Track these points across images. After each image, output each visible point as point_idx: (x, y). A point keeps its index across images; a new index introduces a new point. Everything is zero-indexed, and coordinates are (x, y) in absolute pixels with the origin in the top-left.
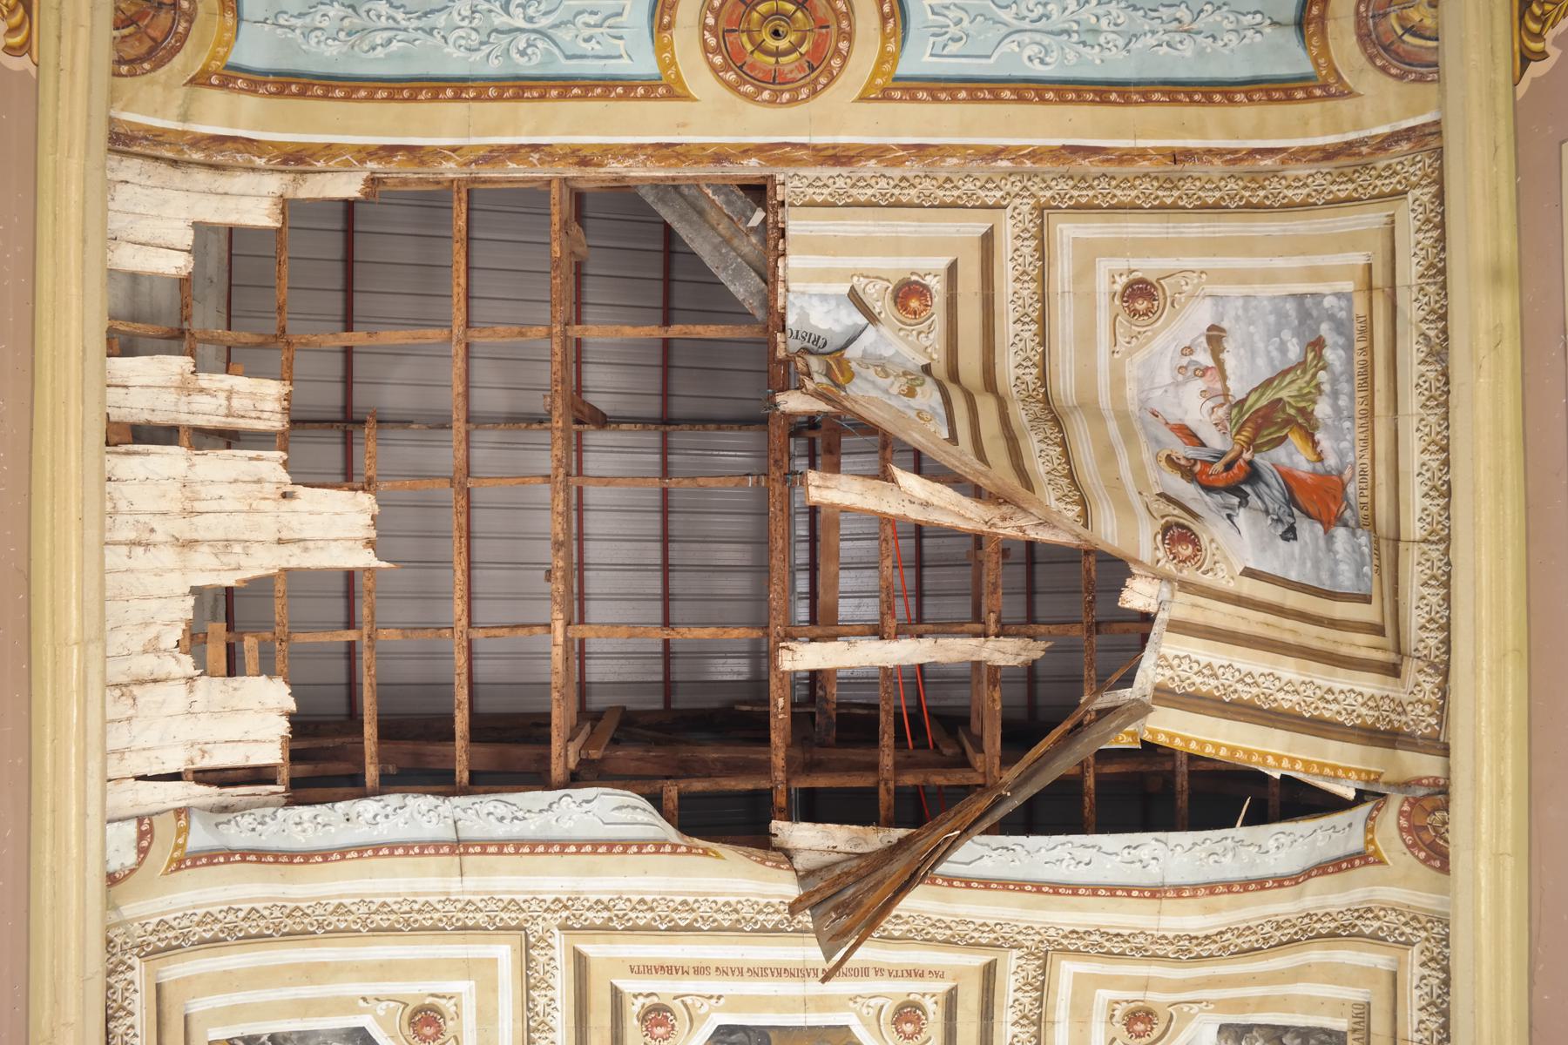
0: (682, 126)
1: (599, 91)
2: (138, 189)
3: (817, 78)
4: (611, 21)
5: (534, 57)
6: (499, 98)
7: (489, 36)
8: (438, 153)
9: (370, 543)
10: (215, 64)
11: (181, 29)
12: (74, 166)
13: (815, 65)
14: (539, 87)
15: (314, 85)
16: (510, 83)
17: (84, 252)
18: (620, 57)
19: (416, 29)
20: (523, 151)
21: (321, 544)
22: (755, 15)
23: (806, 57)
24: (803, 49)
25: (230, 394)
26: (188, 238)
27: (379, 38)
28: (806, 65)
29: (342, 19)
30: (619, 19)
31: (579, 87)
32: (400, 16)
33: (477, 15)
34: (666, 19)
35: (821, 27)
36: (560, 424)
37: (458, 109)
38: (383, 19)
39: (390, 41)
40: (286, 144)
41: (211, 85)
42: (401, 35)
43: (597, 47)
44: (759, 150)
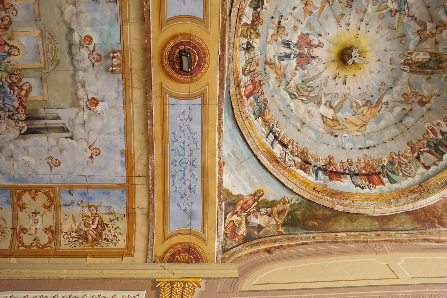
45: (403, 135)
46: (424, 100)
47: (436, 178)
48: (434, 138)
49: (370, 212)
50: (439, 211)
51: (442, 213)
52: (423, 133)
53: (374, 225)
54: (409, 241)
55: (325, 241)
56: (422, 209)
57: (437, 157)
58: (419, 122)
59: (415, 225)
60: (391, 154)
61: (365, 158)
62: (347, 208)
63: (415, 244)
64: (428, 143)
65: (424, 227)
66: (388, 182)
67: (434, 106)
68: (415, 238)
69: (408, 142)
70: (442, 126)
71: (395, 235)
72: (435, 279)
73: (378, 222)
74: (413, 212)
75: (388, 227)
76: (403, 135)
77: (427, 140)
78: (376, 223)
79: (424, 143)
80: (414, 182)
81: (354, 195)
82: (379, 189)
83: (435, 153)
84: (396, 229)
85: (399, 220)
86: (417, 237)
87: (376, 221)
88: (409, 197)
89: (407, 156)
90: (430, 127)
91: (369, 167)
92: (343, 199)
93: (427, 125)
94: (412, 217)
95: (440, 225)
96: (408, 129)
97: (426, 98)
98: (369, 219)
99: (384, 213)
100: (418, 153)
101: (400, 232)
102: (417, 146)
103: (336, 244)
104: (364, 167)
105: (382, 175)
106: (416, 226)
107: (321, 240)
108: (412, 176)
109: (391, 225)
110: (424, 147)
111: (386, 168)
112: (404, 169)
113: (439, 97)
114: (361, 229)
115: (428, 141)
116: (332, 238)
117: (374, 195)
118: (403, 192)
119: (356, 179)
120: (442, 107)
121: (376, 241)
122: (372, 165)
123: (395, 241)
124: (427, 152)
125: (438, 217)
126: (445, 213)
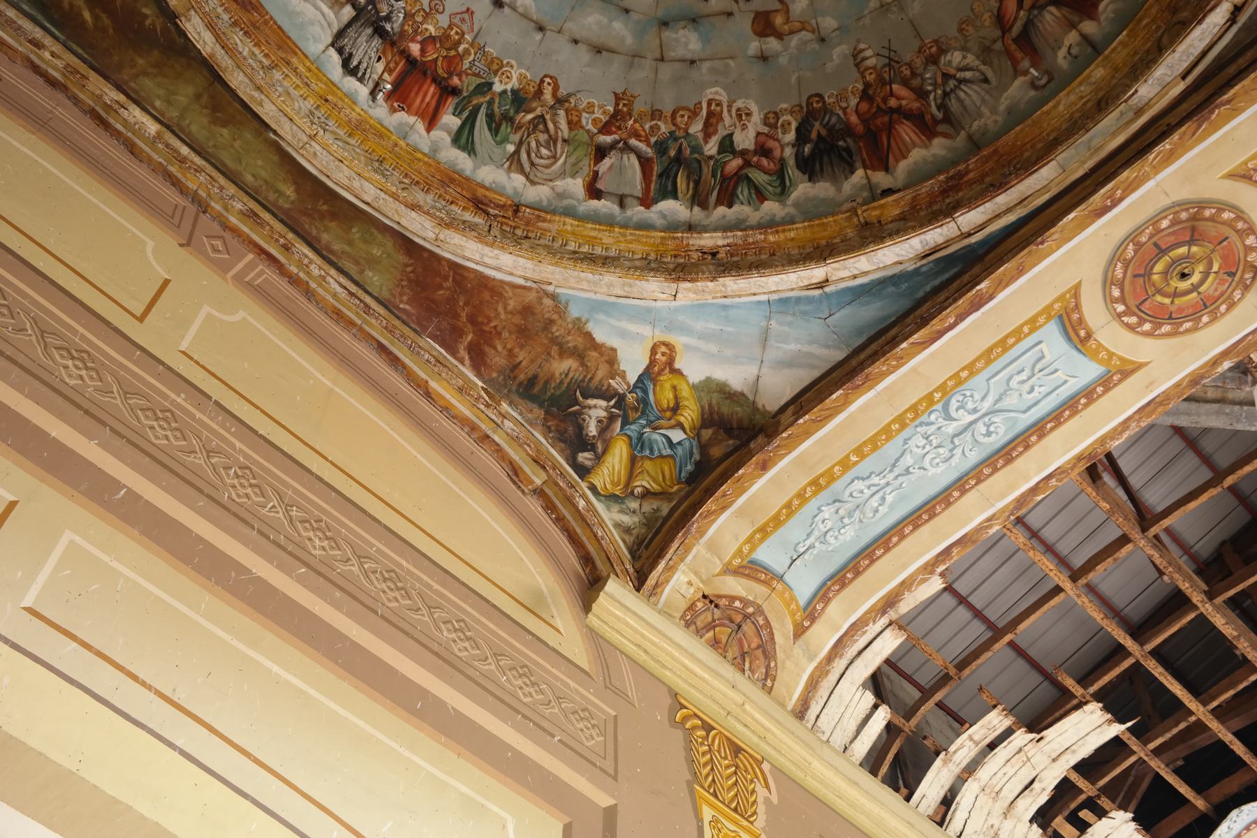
0: (1150, 385)
1: (1067, 413)
2: (825, 711)
3: (1242, 277)
4: (1039, 366)
5: (999, 430)
6: (995, 470)
7: (952, 442)
8: (980, 529)
9: (1110, 722)
10: (798, 617)
11: (761, 622)
12: (816, 765)
13: (1234, 271)
14: (1020, 443)
15: (859, 562)
16: (996, 457)
17: (861, 788)
18: (1066, 382)
19: (896, 478)
20: (1041, 485)
21: (1080, 743)
22: (1155, 277)
23: (1222, 271)
24: (1215, 268)
25: (971, 738)
26: (870, 698)
27: (874, 502)
28: (1225, 276)
29: (837, 512)
30: (1044, 361)
31: (1050, 422)
32: (875, 480)
33: (932, 438)
34: (1082, 333)
35: (1220, 243)
36: (1187, 585)
37: (971, 497)
38: (866, 491)
39: (883, 499)
40: (875, 604)
41: (808, 628)
42: (888, 489)
43: (1042, 389)
44: (1225, 354)
45: (631, 66)
46: (779, 20)
47: (578, 226)
48: (696, 138)
49: (294, 136)
50: (498, 314)
51: (504, 328)
52: (684, 104)
53: (277, 191)
54: (335, 316)
55: (66, 88)
56: (454, 266)
57: (647, 190)
58: (706, 65)
59: (401, 295)
60: (548, 80)
61: (463, 20)
62: (226, 58)
63: (346, 337)
64: (668, 138)
65: (419, 323)
66: (449, 134)
67: (783, 60)
68: (359, 322)
69: (624, 93)
70: (744, 127)
71: (306, 261)
72: (247, 406)
73: (297, 191)
74: (425, 255)
75: (314, 232)
76: (631, 66)
77: (674, 128)
78: (289, 191)
79: (659, 128)
80: (516, 192)
81: (296, 54)
82: (400, 124)
83: (654, 178)
84: (334, 259)
85: (366, 241)
86: (365, 321)
87: (295, 183)
88: (453, 207)
89: (580, 121)
90: (717, 105)
91: (444, 53)
92: (246, 33)
93: (716, 93)
94: (409, 269)
95: (471, 358)
96: (662, 59)
97: (788, 18)
98: (276, 158)
99: (333, 176)
100: (615, 143)
101: (326, 267)
102: (635, 121)
103: (101, 130)
104: (432, 39)
105: (457, 105)
106: (401, 301)
107: (51, 71)
108: (531, 177)
109: (330, 236)
110: (647, 142)
111: (488, 98)
112: (533, 144)
113: (816, 46)
114: (225, 165)
115: (671, 133)
116: (100, 97)
117: (358, 110)
118: (452, 180)
119: (363, 39)
120: (799, 80)
121: (235, 231)
122: (461, 57)
123: (294, 281)
124: (640, 157)
125: (483, 331)
126: (510, 333)
